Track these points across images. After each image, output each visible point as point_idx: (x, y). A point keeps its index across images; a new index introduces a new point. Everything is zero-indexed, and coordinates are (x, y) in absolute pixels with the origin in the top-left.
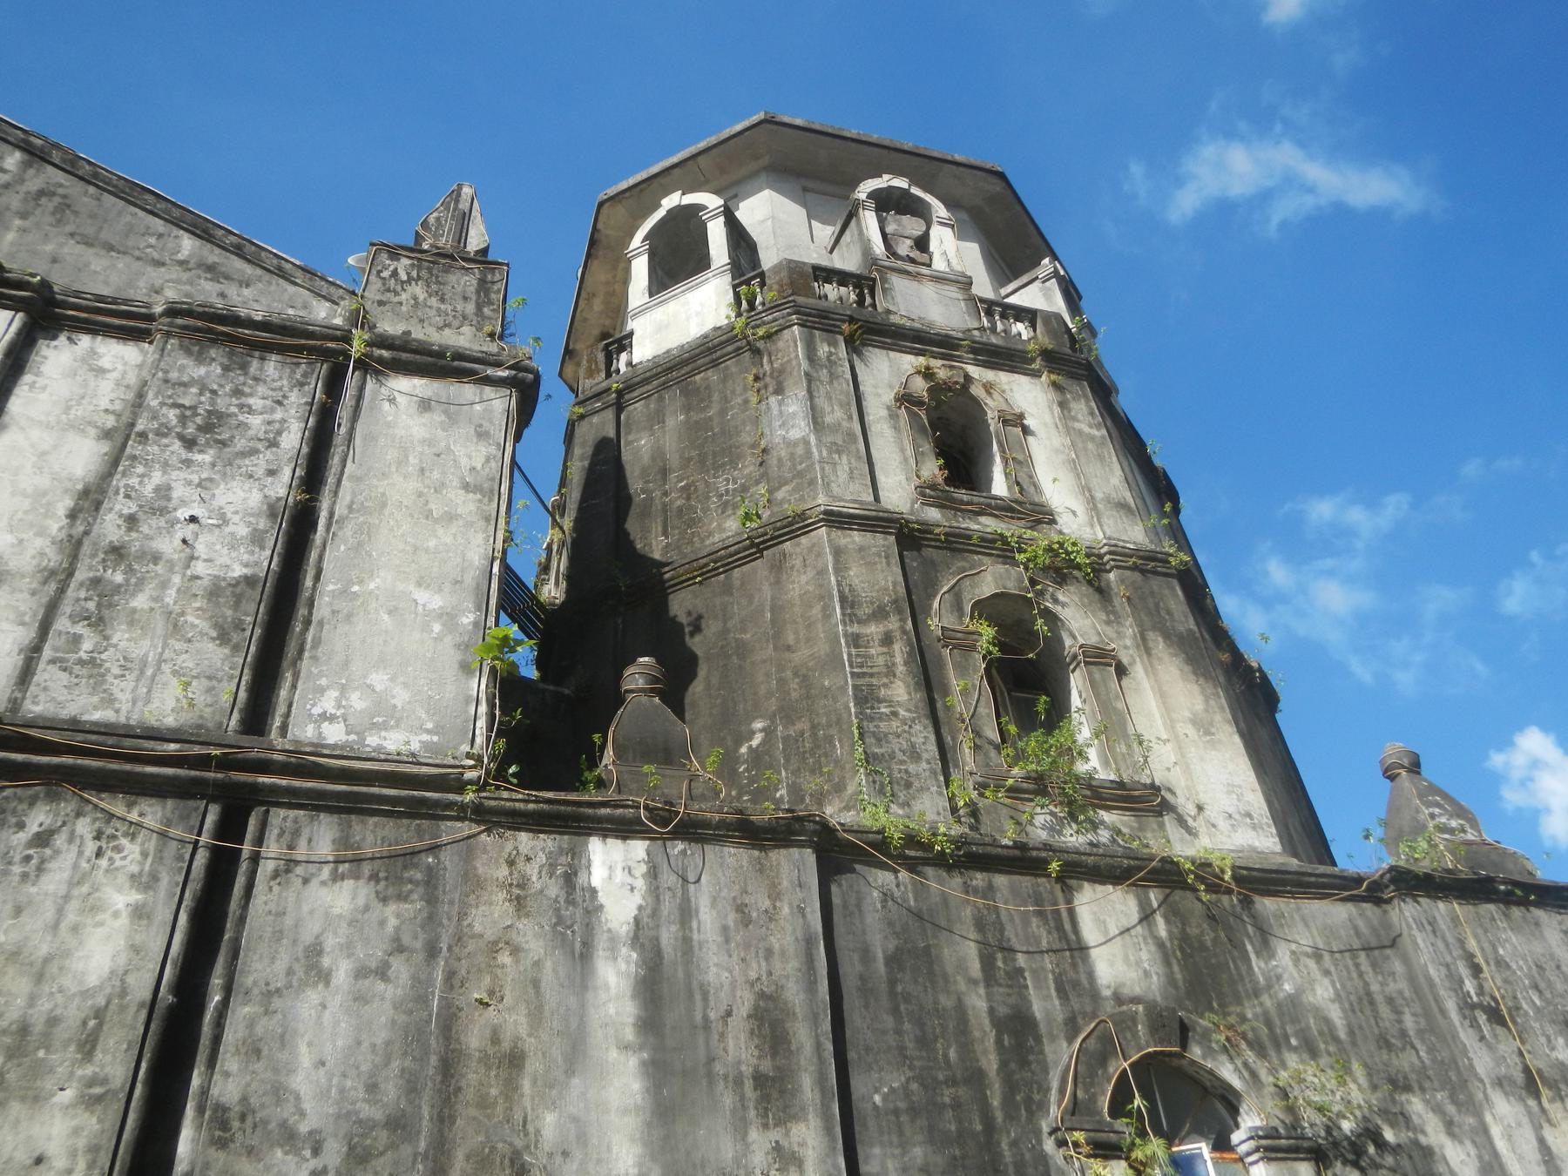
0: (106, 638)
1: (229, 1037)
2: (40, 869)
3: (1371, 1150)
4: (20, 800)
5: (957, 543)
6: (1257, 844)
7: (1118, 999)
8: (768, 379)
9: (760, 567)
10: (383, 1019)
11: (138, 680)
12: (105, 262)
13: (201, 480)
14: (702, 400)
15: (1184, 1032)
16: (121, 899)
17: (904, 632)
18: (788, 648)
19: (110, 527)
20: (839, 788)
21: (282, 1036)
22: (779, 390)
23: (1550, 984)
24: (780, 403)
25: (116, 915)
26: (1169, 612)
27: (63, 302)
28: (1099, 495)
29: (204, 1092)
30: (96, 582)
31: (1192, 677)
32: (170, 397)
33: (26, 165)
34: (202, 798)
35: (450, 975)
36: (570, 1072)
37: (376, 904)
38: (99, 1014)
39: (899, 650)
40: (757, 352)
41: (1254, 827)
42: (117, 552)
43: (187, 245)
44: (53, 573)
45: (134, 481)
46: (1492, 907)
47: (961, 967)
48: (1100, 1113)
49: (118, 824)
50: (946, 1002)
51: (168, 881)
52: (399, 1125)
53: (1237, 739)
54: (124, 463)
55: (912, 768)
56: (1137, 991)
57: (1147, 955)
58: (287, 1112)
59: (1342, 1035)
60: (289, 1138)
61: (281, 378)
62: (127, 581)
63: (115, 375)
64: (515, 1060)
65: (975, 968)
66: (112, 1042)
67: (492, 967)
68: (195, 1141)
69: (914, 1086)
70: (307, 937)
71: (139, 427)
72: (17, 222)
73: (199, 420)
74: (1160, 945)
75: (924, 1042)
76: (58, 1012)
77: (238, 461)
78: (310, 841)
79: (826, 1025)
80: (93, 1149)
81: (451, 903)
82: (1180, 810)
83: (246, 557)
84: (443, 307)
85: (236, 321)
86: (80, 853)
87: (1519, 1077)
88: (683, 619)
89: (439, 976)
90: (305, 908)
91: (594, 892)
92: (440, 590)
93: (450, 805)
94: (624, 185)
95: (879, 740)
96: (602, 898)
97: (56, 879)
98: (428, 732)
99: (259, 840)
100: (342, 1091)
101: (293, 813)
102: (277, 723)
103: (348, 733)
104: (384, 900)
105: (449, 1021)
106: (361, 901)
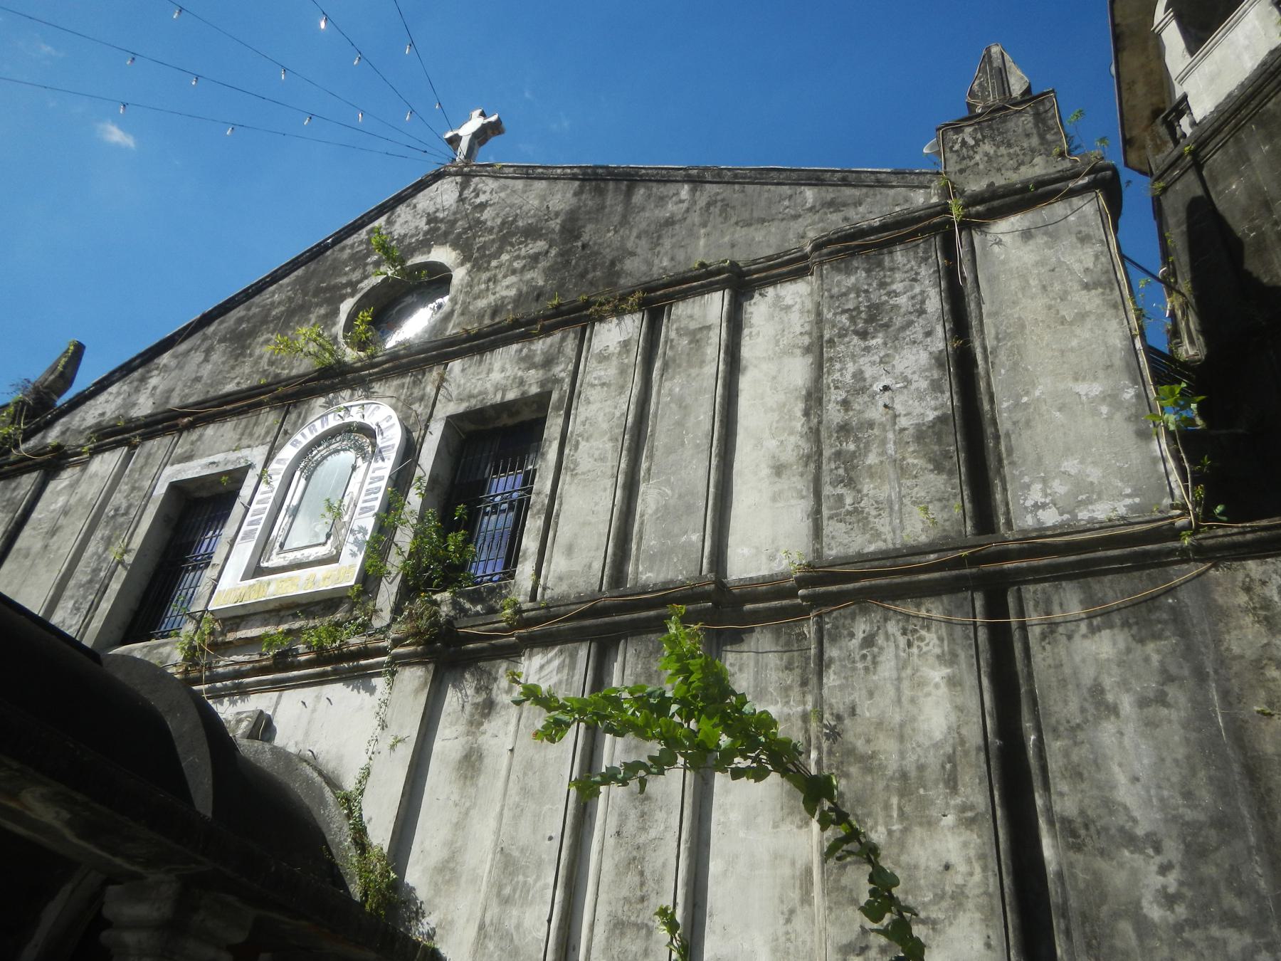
0: (859, 491)
2: (875, 663)
4: (845, 618)
10: (1177, 738)
11: (891, 515)
12: (763, 232)
13: (881, 359)
16: (937, 674)
19: (833, 413)
21: (1095, 761)
25: (937, 686)
27: (749, 270)
29: (1049, 809)
30: (838, 454)
32: (838, 307)
33: (693, 191)
34: (967, 590)
35: (1225, 695)
37: (1134, 645)
38: (951, 758)
42: (844, 430)
43: (810, 194)
44: (809, 457)
45: (837, 375)
49: (915, 621)
52: (1224, 823)
58: (1121, 820)
60: (1130, 840)
61: (909, 261)
62: (858, 447)
63: (797, 306)
66: (967, 778)
67: (1263, 682)
68: (1055, 847)
71: (827, 337)
72: (702, 231)
73: (863, 315)
76: (922, 760)
77: (901, 335)
78: (1061, 605)
80: (982, 857)
81: (1203, 633)
83: (933, 403)
84: (1012, 151)
85: (862, 233)
86: (897, 647)
89: (1215, 696)
90: (1077, 659)
92: (1095, 378)
93: (1171, 552)
97: (887, 668)
98: (1128, 496)
99: (1021, 613)
100: (1162, 800)
101: (1040, 587)
102: (1002, 520)
103: (1061, 514)
104: (1142, 641)
105: (1238, 732)
106: (1122, 645)
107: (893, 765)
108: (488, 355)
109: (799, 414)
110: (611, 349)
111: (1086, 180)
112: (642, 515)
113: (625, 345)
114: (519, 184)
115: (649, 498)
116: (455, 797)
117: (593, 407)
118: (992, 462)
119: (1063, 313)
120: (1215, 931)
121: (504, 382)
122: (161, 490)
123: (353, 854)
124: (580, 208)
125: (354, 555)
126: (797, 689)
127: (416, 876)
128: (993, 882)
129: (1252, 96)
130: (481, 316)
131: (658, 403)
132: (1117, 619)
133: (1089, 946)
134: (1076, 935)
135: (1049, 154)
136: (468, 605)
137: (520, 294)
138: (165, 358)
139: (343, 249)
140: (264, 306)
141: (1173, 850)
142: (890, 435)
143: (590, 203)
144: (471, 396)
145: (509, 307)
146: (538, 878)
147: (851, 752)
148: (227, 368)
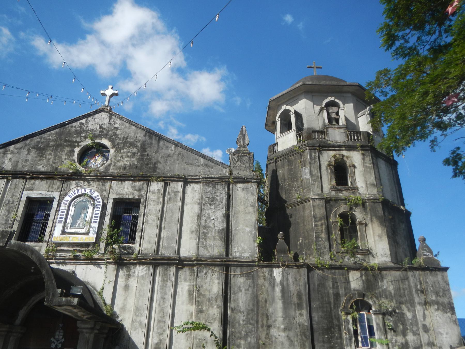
1: (231, 299)
2: (206, 278)
3: (393, 313)
5: (337, 201)
6: (386, 260)
7: (354, 290)
8: (303, 163)
9: (301, 206)
14: (291, 164)
15: (364, 295)
16: (216, 281)
17: (325, 223)
18: (305, 225)
20: (312, 254)
22: (305, 166)
23: (435, 286)
24: (305, 169)
26: (378, 211)
28: (368, 183)
29: (230, 306)
30: (203, 232)
31: (380, 226)
33: (175, 148)
35: (257, 290)
36: (273, 303)
38: (217, 297)
39: (324, 226)
40: (301, 154)
41: (386, 257)
42: (205, 227)
43: (202, 160)
44: (197, 231)
45: (204, 213)
46: (428, 272)
47: (329, 286)
48: (348, 308)
50: (326, 291)
51: (221, 278)
52: (252, 310)
53: (387, 239)
54: (203, 210)
55: (324, 250)
56: (358, 289)
57: (360, 283)
58: (239, 308)
59: (393, 295)
60: (240, 312)
64: (266, 301)
65: (331, 286)
69: (320, 304)
70: (238, 285)
73: (211, 199)
74: (363, 281)
75: (322, 298)
79: (307, 296)
80: (219, 313)
82: (373, 254)
84: (244, 166)
87: (423, 302)
88: (289, 214)
89: (255, 290)
91: (275, 277)
93: (254, 265)
94: (275, 97)
95: (319, 245)
96: (276, 278)
97: (208, 279)
98: (250, 253)
99: (231, 272)
104: (247, 280)
105: (257, 296)
107: (207, 297)
108: (123, 182)
109: (196, 220)
110: (155, 191)
111: (255, 181)
112: (163, 238)
113: (159, 190)
114: (128, 125)
115: (164, 233)
116: (124, 294)
117: (152, 206)
118: (230, 242)
119: (246, 211)
120: (248, 325)
121: (128, 192)
122: (24, 198)
123: (104, 306)
124: (146, 141)
125: (93, 234)
126: (192, 280)
127: (116, 309)
128: (220, 317)
129: (288, 154)
130: (120, 168)
131: (166, 210)
132: (244, 275)
133: (232, 327)
134: (231, 326)
135: (250, 170)
136: (123, 250)
137: (130, 165)
138: (12, 148)
139: (72, 127)
140: (47, 139)
141: (245, 314)
142: (213, 230)
143: (148, 141)
144: (119, 194)
145: (128, 168)
146: (143, 312)
147: (201, 294)
148: (37, 159)
